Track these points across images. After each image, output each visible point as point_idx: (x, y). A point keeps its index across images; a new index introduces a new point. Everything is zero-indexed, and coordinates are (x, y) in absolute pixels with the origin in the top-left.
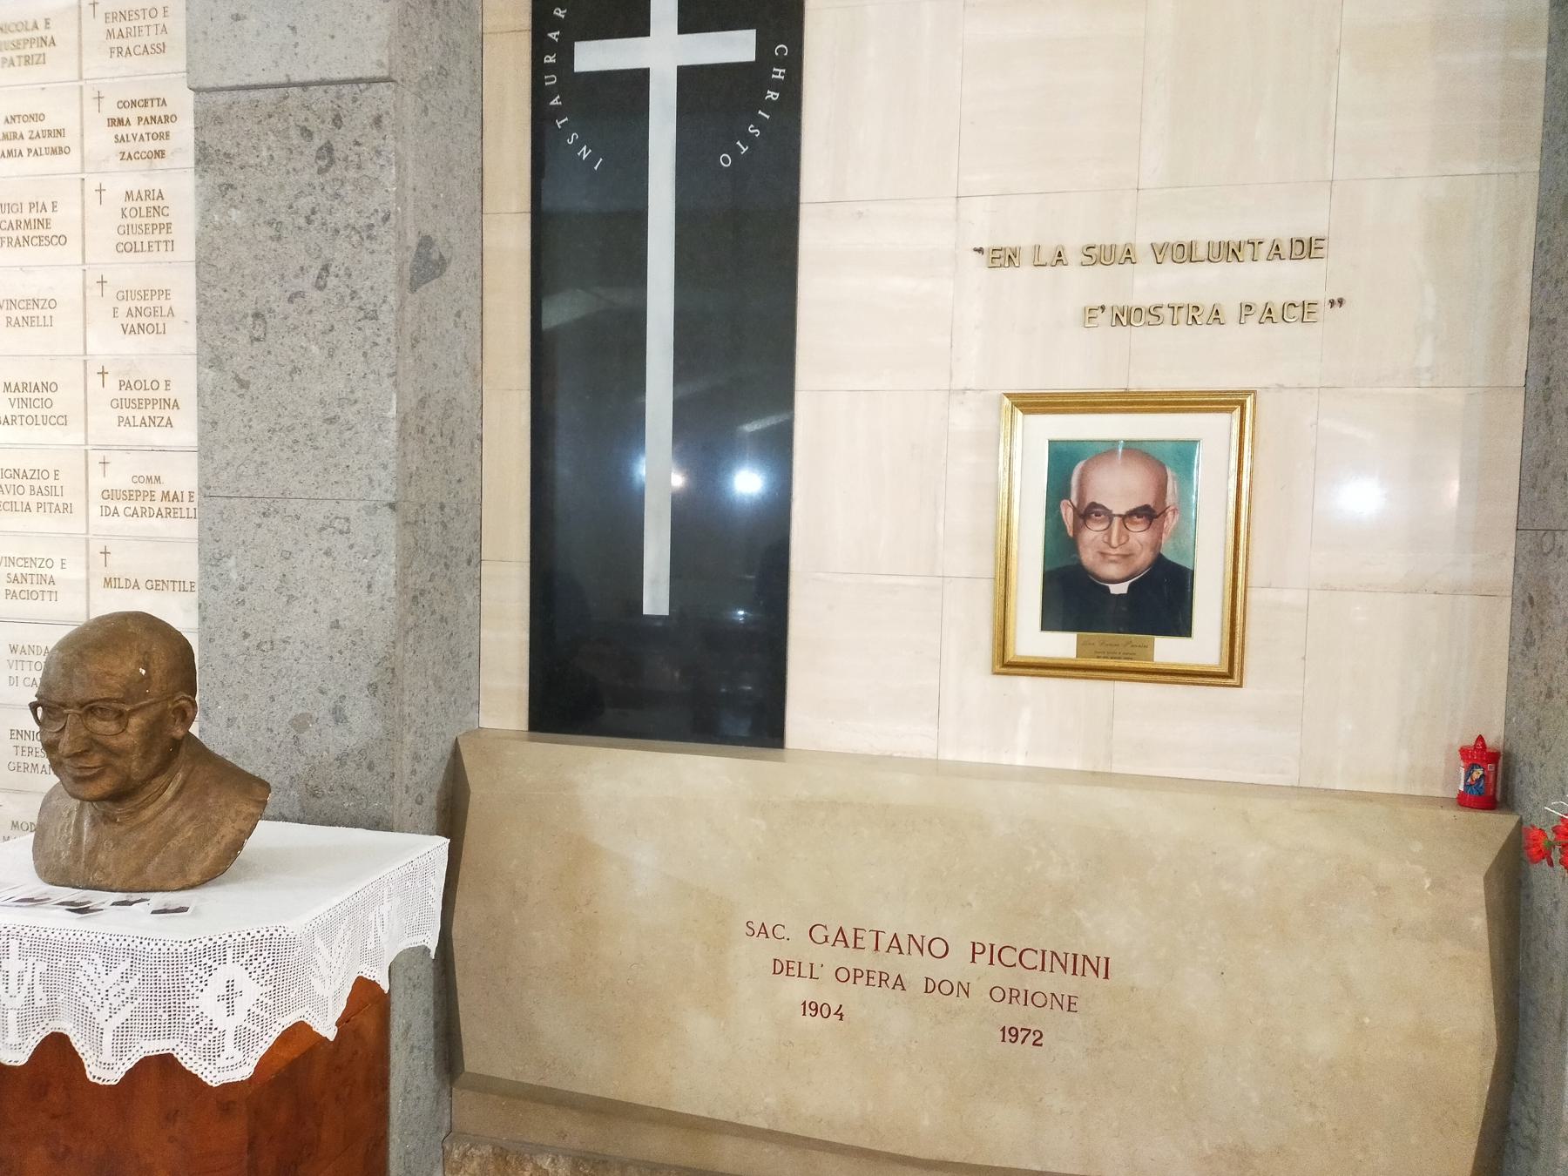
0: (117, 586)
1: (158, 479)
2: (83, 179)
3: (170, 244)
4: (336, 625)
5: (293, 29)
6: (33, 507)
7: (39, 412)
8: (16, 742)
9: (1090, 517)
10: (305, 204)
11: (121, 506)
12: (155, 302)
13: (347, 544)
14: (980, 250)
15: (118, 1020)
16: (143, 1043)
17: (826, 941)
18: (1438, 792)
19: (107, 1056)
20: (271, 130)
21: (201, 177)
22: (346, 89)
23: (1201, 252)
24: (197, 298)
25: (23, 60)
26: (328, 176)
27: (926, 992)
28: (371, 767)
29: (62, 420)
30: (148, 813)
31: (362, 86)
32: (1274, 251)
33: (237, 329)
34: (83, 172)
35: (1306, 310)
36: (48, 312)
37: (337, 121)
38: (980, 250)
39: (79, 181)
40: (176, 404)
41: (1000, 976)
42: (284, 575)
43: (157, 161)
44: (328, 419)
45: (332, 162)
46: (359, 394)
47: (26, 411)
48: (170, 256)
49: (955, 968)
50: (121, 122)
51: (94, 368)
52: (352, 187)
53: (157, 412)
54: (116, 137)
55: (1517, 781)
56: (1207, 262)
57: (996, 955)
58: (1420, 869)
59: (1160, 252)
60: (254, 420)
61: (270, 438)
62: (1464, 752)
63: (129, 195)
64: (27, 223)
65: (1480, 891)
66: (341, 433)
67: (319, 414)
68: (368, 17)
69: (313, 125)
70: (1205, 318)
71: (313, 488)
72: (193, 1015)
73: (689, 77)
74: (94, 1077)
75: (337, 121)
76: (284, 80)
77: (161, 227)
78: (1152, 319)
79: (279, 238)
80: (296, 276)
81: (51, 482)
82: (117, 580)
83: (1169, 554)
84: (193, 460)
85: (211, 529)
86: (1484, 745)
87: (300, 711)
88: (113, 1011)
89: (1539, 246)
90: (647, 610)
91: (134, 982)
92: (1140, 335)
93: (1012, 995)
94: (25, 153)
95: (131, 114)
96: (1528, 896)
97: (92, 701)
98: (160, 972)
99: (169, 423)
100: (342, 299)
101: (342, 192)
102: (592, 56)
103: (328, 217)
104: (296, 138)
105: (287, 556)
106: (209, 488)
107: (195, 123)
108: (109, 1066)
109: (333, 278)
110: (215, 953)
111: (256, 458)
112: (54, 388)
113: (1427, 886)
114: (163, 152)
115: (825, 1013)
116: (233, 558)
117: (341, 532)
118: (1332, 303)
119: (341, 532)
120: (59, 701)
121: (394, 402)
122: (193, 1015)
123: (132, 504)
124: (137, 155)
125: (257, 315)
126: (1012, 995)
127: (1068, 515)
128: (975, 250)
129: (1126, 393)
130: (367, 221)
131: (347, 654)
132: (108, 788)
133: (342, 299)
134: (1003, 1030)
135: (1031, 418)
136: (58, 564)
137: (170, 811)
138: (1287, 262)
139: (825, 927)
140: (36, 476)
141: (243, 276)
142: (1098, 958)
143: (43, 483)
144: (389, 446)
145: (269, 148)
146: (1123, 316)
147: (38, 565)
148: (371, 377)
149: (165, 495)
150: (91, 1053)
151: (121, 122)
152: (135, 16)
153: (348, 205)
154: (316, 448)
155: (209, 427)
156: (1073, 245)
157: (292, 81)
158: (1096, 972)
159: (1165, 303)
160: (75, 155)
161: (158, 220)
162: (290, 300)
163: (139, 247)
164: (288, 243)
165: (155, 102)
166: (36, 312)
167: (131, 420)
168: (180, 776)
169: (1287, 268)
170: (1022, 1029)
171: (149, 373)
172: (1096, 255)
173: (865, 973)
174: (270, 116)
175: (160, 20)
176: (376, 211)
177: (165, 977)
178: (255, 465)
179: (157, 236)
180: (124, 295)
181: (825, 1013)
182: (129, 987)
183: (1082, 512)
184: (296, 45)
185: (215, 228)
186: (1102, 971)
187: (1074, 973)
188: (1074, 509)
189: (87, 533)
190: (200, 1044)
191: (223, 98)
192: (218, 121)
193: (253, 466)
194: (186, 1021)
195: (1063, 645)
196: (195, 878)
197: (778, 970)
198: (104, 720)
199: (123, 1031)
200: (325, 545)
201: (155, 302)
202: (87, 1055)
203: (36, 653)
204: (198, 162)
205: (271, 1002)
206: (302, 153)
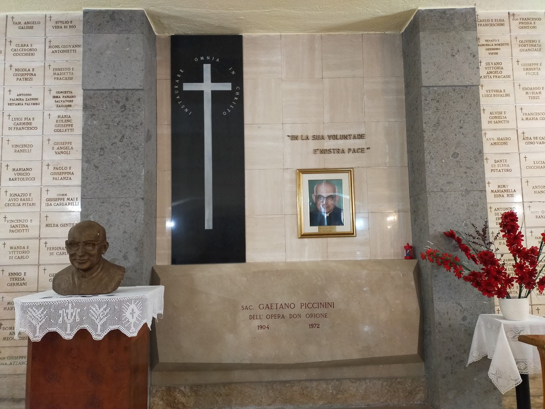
0: (50, 226)
1: (66, 195)
2: (44, 112)
3: (72, 130)
4: (125, 232)
5: (115, 76)
6: (21, 204)
7: (25, 177)
8: (11, 277)
9: (319, 198)
10: (117, 120)
11: (53, 203)
12: (67, 145)
13: (129, 209)
14: (289, 136)
15: (102, 322)
16: (110, 327)
17: (263, 308)
18: (400, 258)
19: (99, 332)
20: (107, 101)
21: (85, 112)
22: (130, 92)
23: (339, 137)
24: (82, 144)
25: (24, 79)
26: (124, 113)
27: (290, 318)
28: (135, 271)
29: (33, 179)
30: (94, 275)
31: (134, 91)
32: (354, 137)
33: (95, 152)
34: (44, 110)
35: (362, 150)
36: (30, 148)
37: (127, 99)
38: (289, 136)
39: (42, 113)
40: (73, 174)
41: (308, 311)
42: (109, 219)
43: (69, 108)
44: (123, 176)
45: (125, 109)
46: (133, 169)
47: (20, 177)
48: (72, 133)
49: (297, 311)
50: (57, 97)
51: (45, 164)
52: (131, 116)
53: (66, 176)
54: (55, 101)
55: (416, 252)
56: (340, 140)
57: (307, 306)
58: (400, 272)
59: (330, 137)
60: (100, 177)
61: (105, 182)
62: (405, 247)
63: (59, 117)
64: (24, 124)
65: (412, 275)
66: (127, 179)
67: (120, 174)
68: (137, 74)
69: (119, 100)
70: (341, 152)
71: (118, 195)
72: (124, 318)
73: (215, 94)
74: (95, 338)
75: (127, 99)
76: (112, 88)
77: (69, 125)
78: (329, 152)
79: (109, 128)
80: (114, 138)
81: (28, 197)
82: (50, 225)
83: (337, 205)
84: (80, 188)
85: (85, 208)
86: (409, 245)
87: (113, 258)
88: (101, 319)
89: (407, 136)
90: (206, 228)
91: (108, 311)
92: (327, 156)
93: (311, 316)
94: (24, 104)
95: (61, 95)
96: (422, 276)
97: (87, 241)
98: (116, 307)
99: (70, 179)
100: (128, 145)
101: (128, 117)
102: (188, 87)
103: (124, 123)
104: (114, 103)
105: (110, 214)
106: (85, 196)
107: (83, 98)
108: (99, 335)
109: (125, 139)
110: (130, 301)
111: (100, 187)
112: (30, 170)
113: (402, 276)
114: (71, 105)
115: (264, 328)
116: (92, 215)
117: (127, 206)
118: (367, 148)
119: (127, 206)
120: (77, 241)
121: (143, 171)
122: (124, 318)
123: (57, 202)
124: (62, 106)
125: (101, 149)
126: (311, 316)
127: (314, 198)
128: (288, 136)
129: (325, 169)
130: (136, 125)
131: (128, 240)
132: (88, 266)
133: (128, 145)
134: (310, 325)
135: (303, 175)
136: (29, 221)
137: (101, 274)
138: (357, 139)
139: (263, 304)
140: (23, 195)
141: (97, 138)
142: (331, 303)
143: (25, 197)
144: (142, 183)
145: (106, 105)
146: (323, 151)
147: (22, 222)
148: (137, 165)
149: (68, 199)
150: (94, 332)
151: (57, 97)
152: (63, 70)
153: (130, 120)
154: (120, 184)
155: (85, 179)
156: (310, 135)
157: (115, 88)
158: (331, 306)
159: (332, 148)
160: (41, 105)
161: (68, 123)
162: (112, 145)
163: (62, 131)
164: (112, 130)
165: (69, 92)
166: (25, 148)
167: (57, 178)
168: (101, 265)
169: (357, 141)
170: (315, 324)
171: (64, 165)
172: (315, 138)
173: (274, 315)
174: (107, 97)
175: (71, 71)
176: (138, 122)
177: (117, 308)
178: (100, 189)
179: (68, 128)
180: (56, 144)
181: (264, 328)
182: (106, 312)
183: (317, 197)
184: (116, 80)
185: (89, 125)
186: (332, 306)
187: (326, 308)
188: (315, 196)
189: (40, 211)
190: (126, 326)
191: (92, 92)
192: (91, 98)
193: (99, 189)
194: (122, 320)
195: (315, 229)
196: (110, 291)
197: (251, 318)
198: (89, 246)
199: (104, 326)
200: (122, 210)
201: (67, 145)
202: (93, 333)
203: (20, 248)
204: (84, 108)
205: (141, 316)
206: (116, 107)
